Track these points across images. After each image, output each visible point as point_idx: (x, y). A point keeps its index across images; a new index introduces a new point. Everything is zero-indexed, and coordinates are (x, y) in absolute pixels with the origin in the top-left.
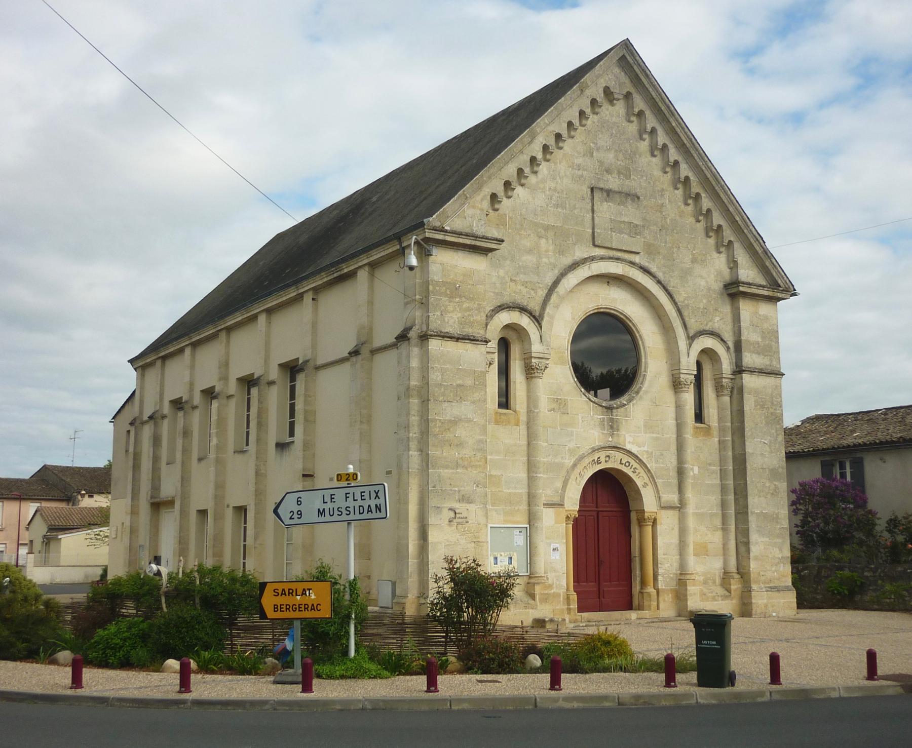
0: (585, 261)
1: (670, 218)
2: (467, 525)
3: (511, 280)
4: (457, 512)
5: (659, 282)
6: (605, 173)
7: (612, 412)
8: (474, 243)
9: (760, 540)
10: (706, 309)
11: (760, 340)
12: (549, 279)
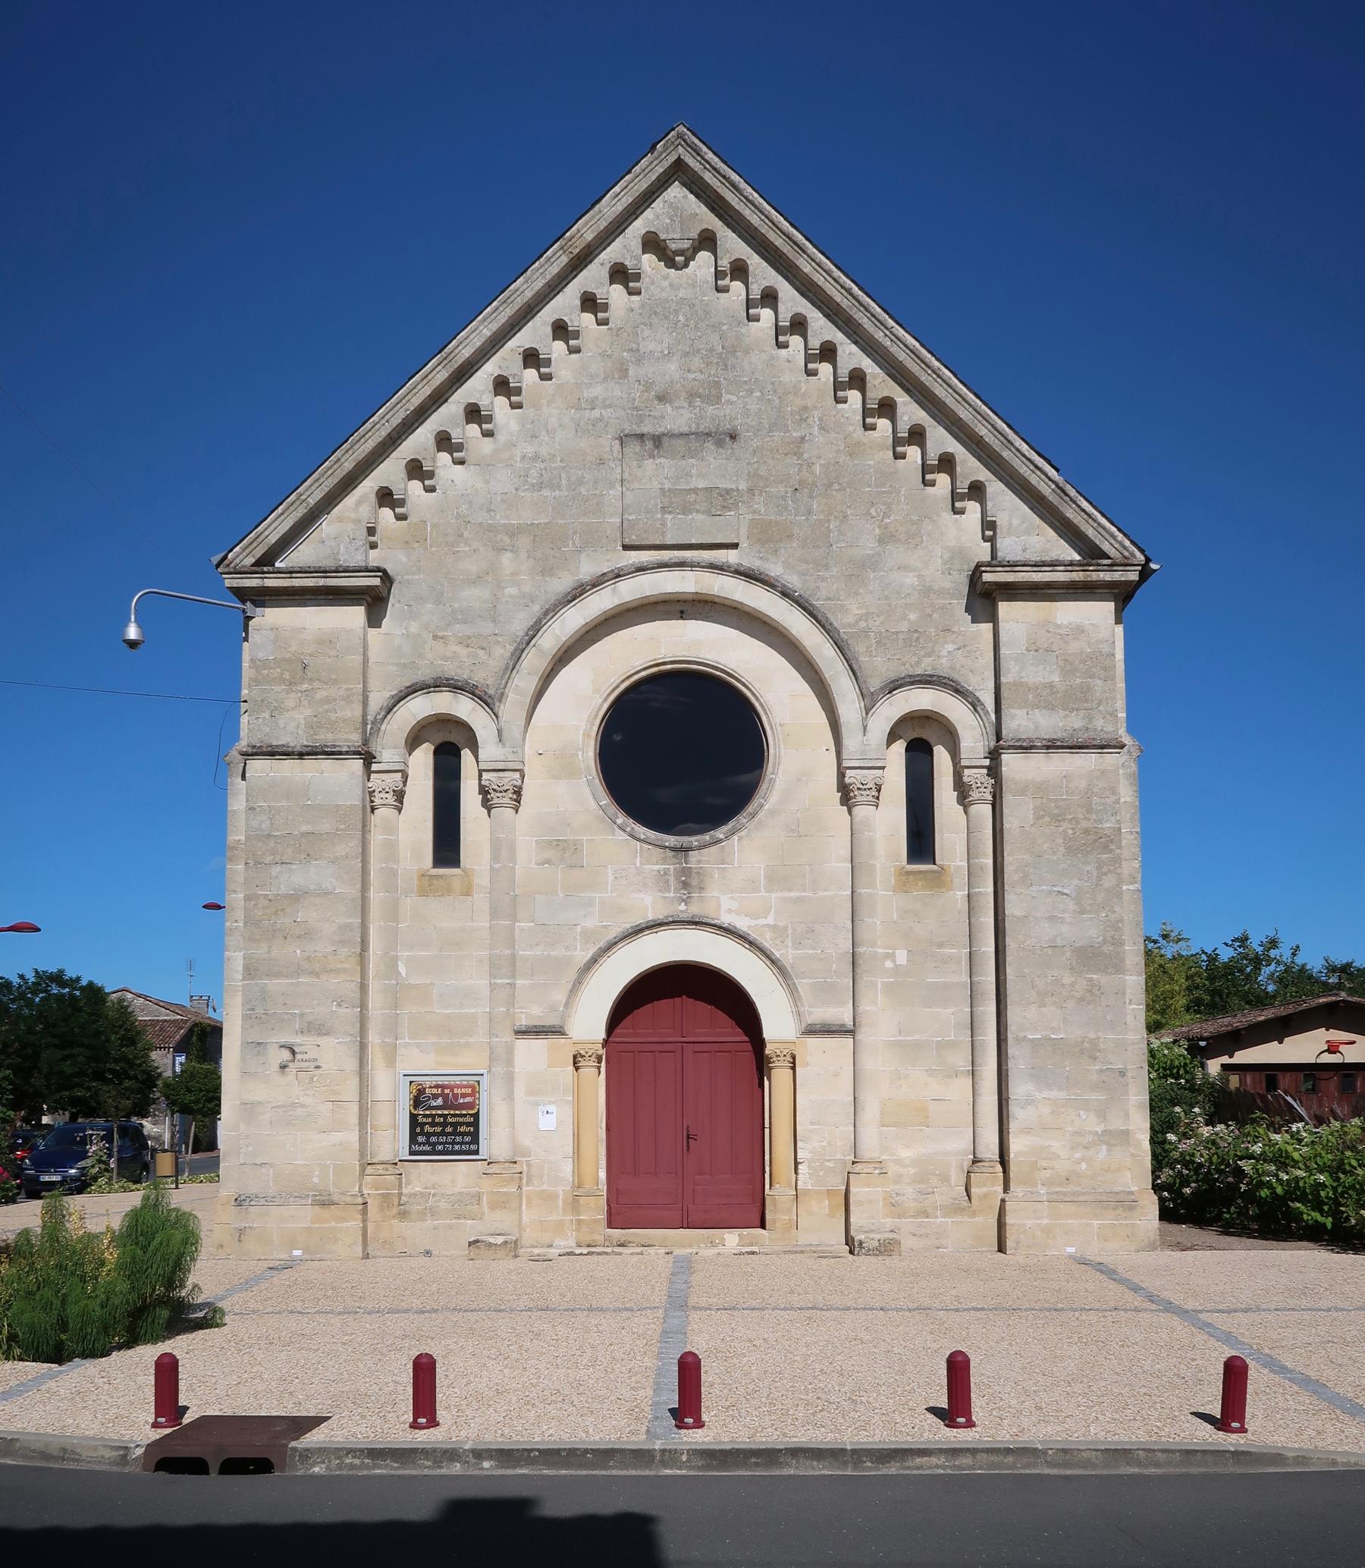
0: (597, 583)
1: (822, 461)
2: (320, 1071)
3: (435, 637)
4: (297, 1049)
5: (785, 594)
6: (656, 402)
7: (686, 856)
8: (321, 582)
9: (1038, 1096)
11: (1056, 678)
12: (519, 624)
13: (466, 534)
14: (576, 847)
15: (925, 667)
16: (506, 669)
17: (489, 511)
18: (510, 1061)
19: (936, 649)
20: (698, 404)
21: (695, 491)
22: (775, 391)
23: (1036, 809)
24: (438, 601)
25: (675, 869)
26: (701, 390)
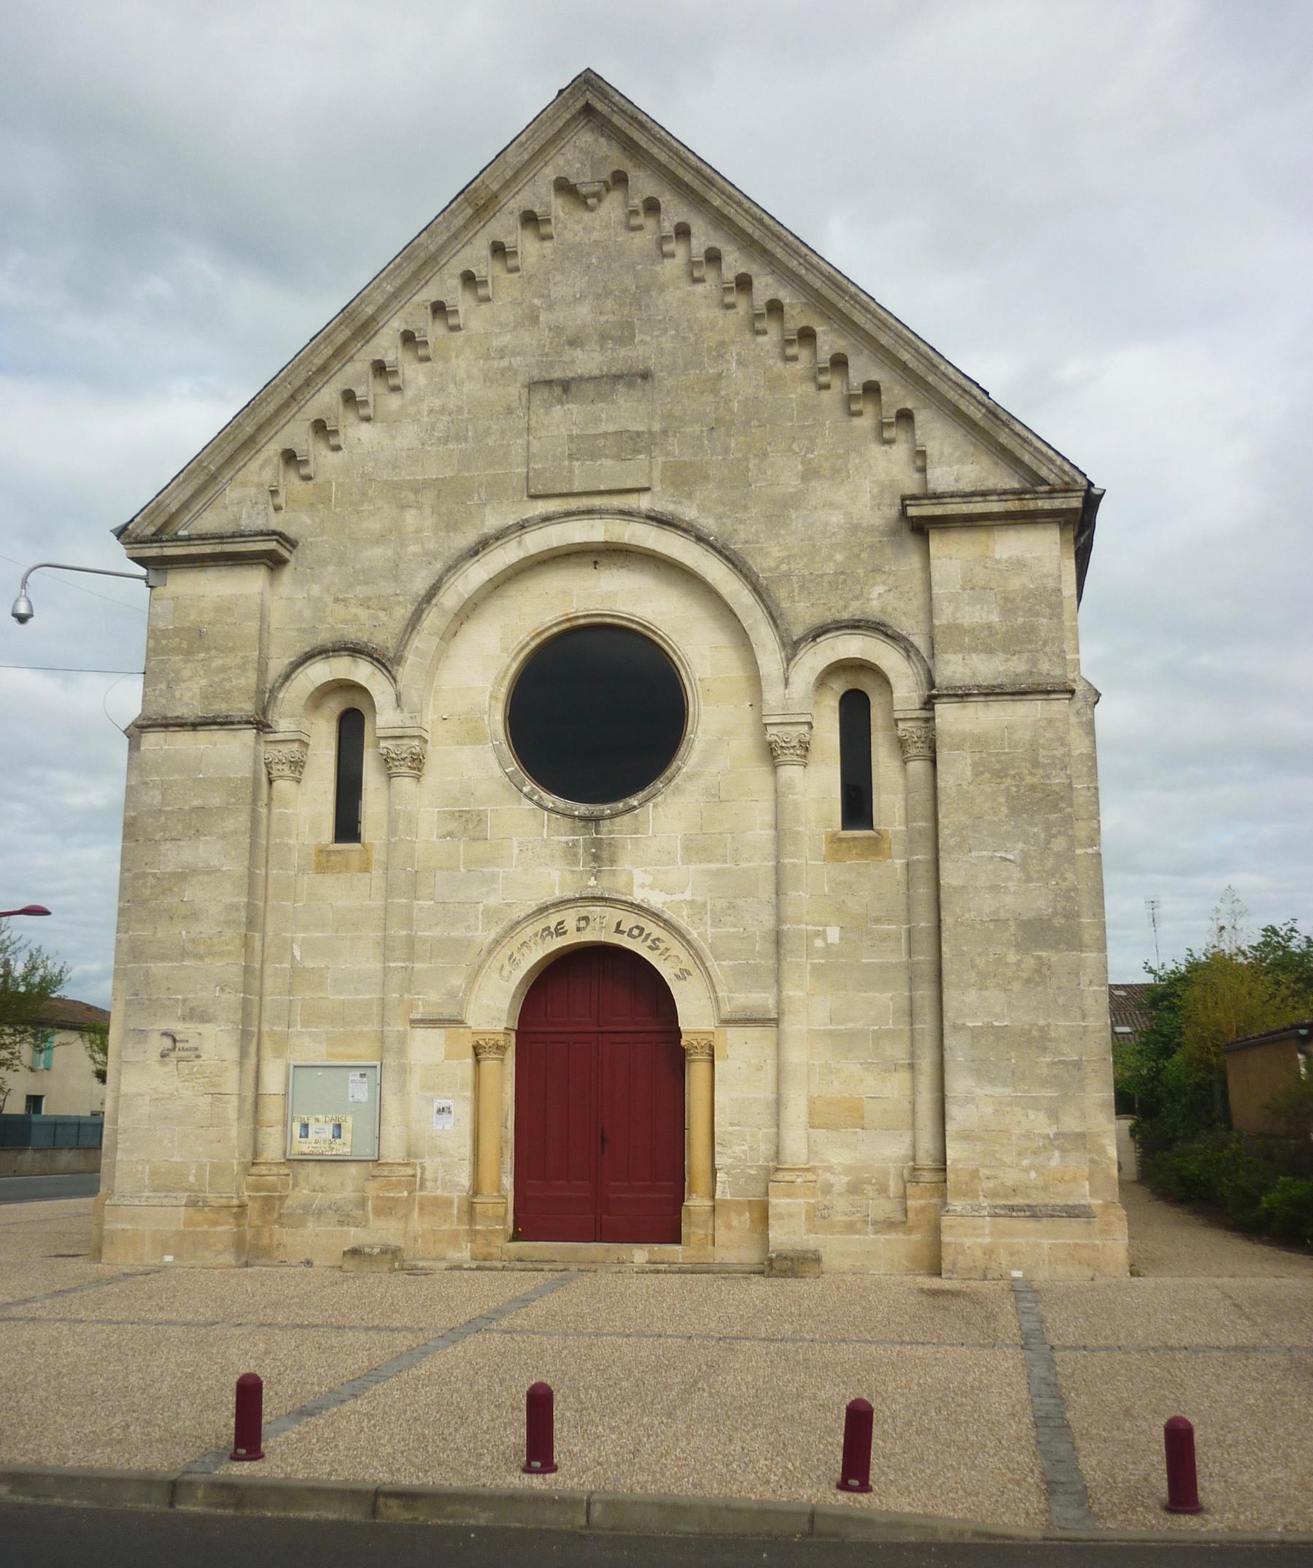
0: (501, 535)
1: (740, 398)
3: (336, 600)
5: (700, 539)
6: (566, 347)
7: (597, 826)
9: (979, 1092)
10: (842, 573)
11: (995, 618)
12: (420, 584)
13: (370, 492)
14: (480, 818)
15: (853, 610)
16: (406, 630)
17: (395, 467)
18: (402, 1052)
19: (865, 590)
20: (610, 346)
21: (605, 435)
22: (691, 328)
23: (974, 764)
24: (341, 562)
25: (584, 839)
26: (613, 332)
